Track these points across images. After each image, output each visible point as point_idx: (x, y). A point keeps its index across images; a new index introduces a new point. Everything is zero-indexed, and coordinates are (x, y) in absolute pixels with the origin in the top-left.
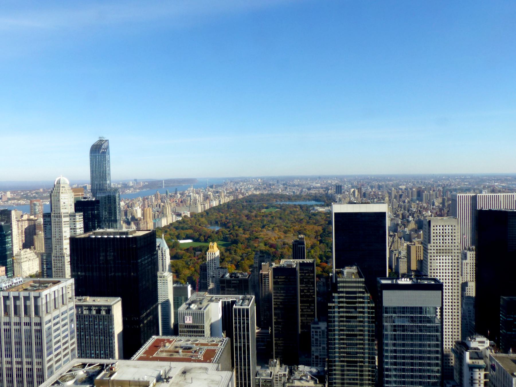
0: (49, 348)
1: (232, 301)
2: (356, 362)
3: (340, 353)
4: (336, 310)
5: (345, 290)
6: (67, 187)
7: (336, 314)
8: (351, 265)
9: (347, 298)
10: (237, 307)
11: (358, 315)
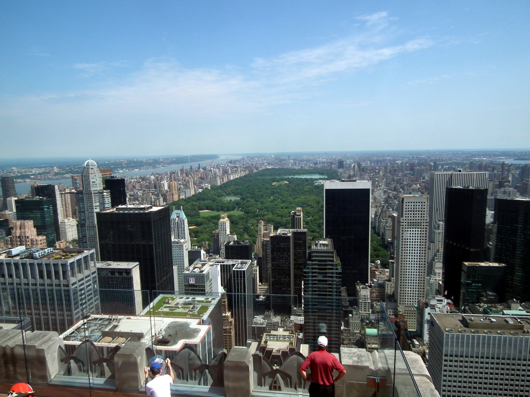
0: (76, 303)
2: (326, 316)
3: (312, 309)
4: (310, 274)
5: (317, 258)
6: (96, 169)
7: (310, 278)
9: (319, 265)
11: (328, 279)
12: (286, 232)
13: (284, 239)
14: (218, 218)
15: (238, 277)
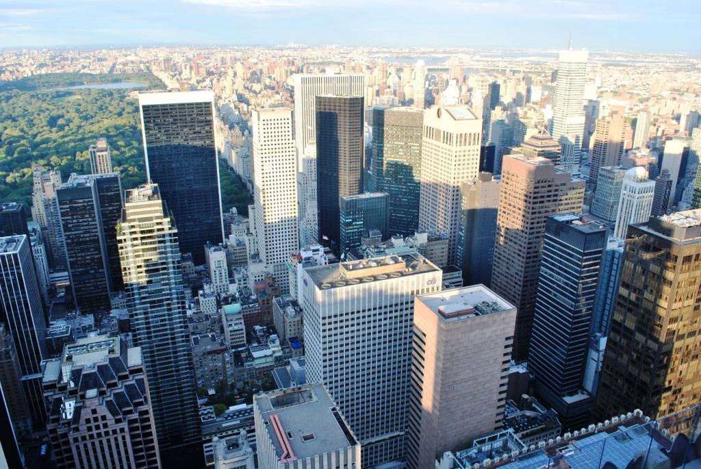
3: (140, 294)
5: (136, 217)
13: (82, 190)
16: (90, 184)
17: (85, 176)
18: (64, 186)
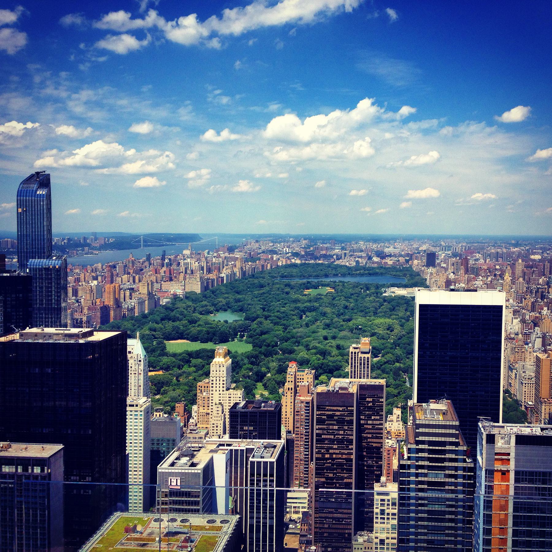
1: (247, 449)
5: (426, 439)
7: (413, 478)
8: (437, 397)
10: (255, 460)
12: (346, 385)
14: (210, 355)
15: (259, 474)
16: (353, 390)
17: (348, 380)
18: (321, 389)
